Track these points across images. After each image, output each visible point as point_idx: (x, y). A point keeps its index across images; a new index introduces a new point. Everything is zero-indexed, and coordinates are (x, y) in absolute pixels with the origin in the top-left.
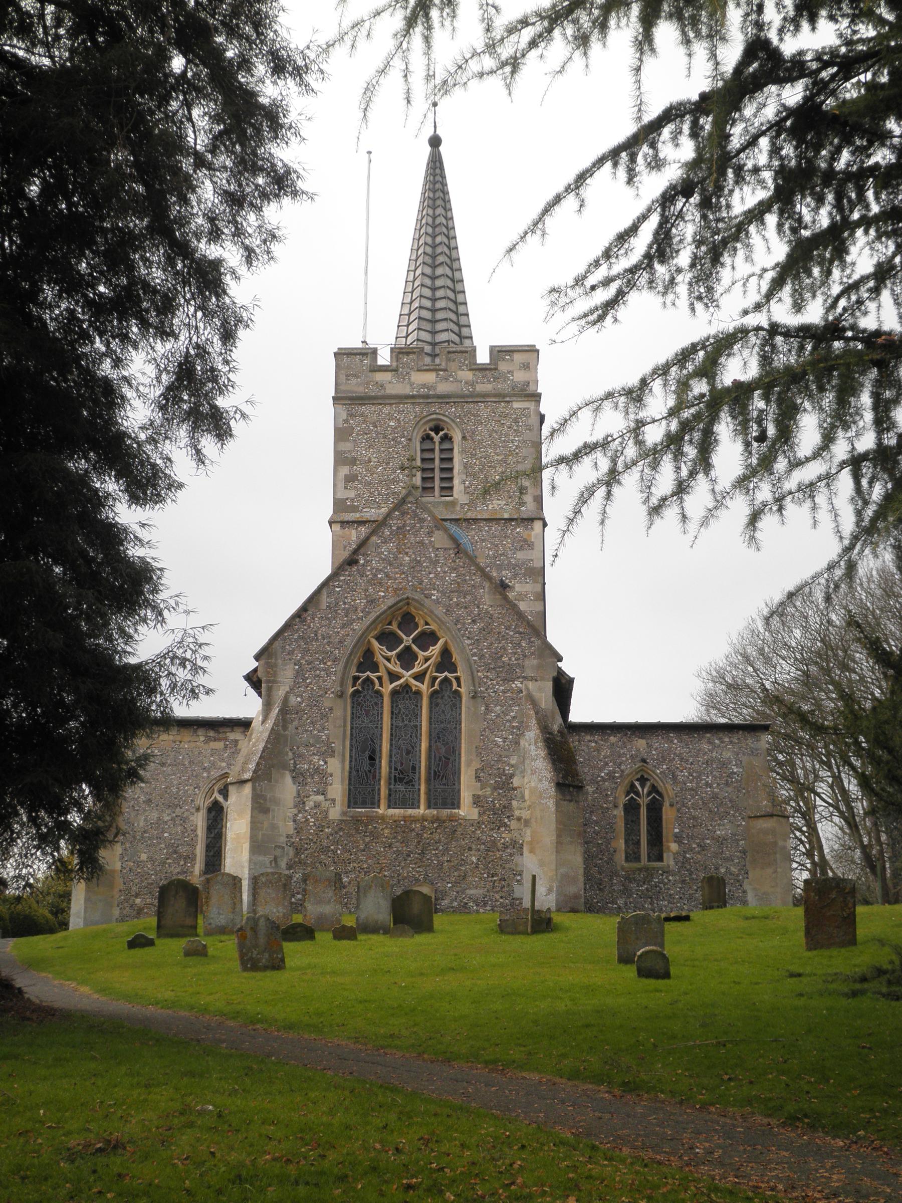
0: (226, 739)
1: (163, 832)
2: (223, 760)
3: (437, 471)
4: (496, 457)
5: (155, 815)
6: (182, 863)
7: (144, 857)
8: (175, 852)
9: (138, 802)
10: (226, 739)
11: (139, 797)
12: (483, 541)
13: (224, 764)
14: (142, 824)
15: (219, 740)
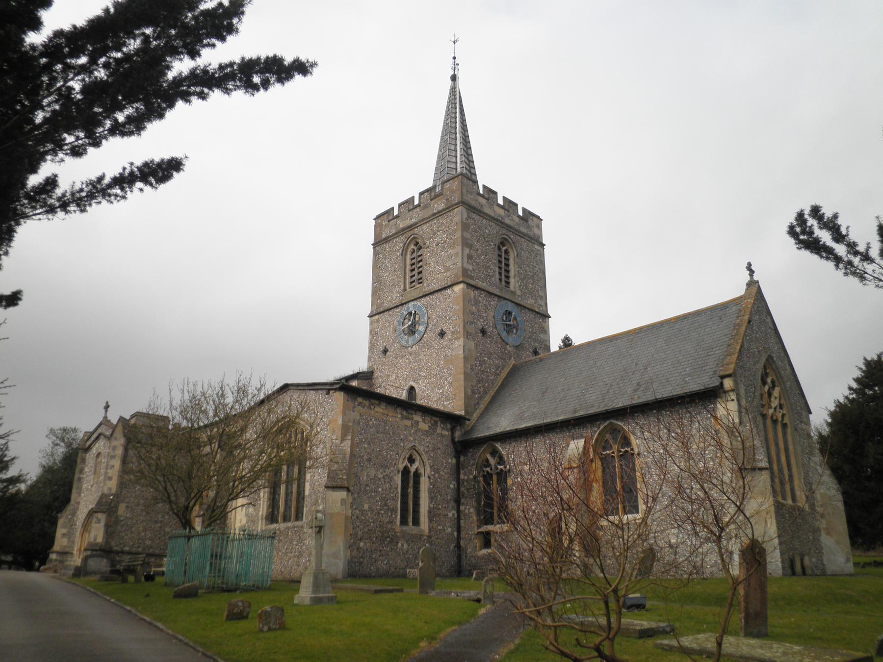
0: (412, 419)
1: (378, 487)
2: (411, 435)
3: (503, 270)
4: (530, 273)
5: (372, 472)
6: (390, 514)
7: (366, 507)
8: (386, 505)
9: (363, 459)
10: (412, 419)
11: (363, 456)
12: (527, 321)
13: (412, 439)
14: (365, 478)
15: (408, 419)
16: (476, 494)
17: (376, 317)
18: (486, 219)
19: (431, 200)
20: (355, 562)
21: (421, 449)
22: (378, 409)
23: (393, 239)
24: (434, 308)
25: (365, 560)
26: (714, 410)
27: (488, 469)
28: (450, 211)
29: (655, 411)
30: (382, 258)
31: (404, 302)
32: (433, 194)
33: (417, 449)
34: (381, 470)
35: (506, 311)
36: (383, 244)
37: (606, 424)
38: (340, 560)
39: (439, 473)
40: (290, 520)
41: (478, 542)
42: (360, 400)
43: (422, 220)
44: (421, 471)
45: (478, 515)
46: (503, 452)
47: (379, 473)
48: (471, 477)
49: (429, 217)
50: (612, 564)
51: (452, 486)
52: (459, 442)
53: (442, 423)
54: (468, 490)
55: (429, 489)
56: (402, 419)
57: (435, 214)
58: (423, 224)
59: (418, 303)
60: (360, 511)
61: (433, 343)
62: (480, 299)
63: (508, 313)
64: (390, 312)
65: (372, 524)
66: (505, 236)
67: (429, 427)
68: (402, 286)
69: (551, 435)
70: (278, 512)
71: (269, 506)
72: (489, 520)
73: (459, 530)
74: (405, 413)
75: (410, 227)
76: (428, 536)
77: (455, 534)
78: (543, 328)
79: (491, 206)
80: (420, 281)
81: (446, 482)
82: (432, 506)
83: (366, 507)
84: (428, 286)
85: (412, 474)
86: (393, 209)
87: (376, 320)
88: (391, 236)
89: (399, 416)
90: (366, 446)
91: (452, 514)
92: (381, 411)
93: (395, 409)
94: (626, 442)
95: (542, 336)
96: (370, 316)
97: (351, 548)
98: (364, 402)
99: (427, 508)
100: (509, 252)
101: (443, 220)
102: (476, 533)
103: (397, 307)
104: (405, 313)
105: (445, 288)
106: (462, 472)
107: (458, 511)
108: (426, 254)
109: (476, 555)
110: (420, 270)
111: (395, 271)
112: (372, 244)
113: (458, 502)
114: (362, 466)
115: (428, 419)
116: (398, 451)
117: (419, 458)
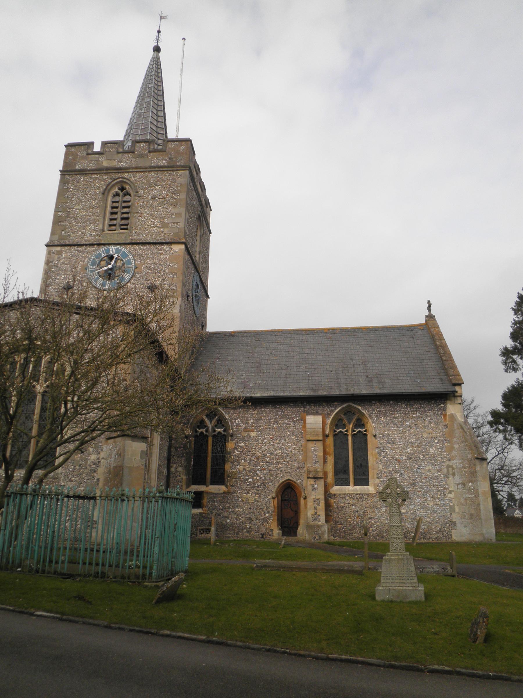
16: (187, 453)
19: (150, 152)
23: (92, 174)
24: (143, 259)
26: (444, 409)
27: (204, 430)
28: (173, 171)
29: (391, 402)
30: (73, 189)
31: (102, 242)
32: (152, 147)
36: (76, 174)
37: (344, 406)
43: (136, 168)
45: (187, 474)
46: (226, 417)
49: (146, 168)
50: (343, 528)
57: (154, 167)
59: (123, 249)
64: (80, 249)
68: (101, 226)
75: (119, 170)
80: (125, 227)
84: (138, 235)
86: (92, 143)
87: (58, 252)
88: (89, 170)
94: (360, 423)
96: (47, 246)
101: (165, 177)
103: (92, 245)
104: (103, 255)
105: (162, 243)
108: (138, 204)
111: (91, 207)
112: (61, 171)
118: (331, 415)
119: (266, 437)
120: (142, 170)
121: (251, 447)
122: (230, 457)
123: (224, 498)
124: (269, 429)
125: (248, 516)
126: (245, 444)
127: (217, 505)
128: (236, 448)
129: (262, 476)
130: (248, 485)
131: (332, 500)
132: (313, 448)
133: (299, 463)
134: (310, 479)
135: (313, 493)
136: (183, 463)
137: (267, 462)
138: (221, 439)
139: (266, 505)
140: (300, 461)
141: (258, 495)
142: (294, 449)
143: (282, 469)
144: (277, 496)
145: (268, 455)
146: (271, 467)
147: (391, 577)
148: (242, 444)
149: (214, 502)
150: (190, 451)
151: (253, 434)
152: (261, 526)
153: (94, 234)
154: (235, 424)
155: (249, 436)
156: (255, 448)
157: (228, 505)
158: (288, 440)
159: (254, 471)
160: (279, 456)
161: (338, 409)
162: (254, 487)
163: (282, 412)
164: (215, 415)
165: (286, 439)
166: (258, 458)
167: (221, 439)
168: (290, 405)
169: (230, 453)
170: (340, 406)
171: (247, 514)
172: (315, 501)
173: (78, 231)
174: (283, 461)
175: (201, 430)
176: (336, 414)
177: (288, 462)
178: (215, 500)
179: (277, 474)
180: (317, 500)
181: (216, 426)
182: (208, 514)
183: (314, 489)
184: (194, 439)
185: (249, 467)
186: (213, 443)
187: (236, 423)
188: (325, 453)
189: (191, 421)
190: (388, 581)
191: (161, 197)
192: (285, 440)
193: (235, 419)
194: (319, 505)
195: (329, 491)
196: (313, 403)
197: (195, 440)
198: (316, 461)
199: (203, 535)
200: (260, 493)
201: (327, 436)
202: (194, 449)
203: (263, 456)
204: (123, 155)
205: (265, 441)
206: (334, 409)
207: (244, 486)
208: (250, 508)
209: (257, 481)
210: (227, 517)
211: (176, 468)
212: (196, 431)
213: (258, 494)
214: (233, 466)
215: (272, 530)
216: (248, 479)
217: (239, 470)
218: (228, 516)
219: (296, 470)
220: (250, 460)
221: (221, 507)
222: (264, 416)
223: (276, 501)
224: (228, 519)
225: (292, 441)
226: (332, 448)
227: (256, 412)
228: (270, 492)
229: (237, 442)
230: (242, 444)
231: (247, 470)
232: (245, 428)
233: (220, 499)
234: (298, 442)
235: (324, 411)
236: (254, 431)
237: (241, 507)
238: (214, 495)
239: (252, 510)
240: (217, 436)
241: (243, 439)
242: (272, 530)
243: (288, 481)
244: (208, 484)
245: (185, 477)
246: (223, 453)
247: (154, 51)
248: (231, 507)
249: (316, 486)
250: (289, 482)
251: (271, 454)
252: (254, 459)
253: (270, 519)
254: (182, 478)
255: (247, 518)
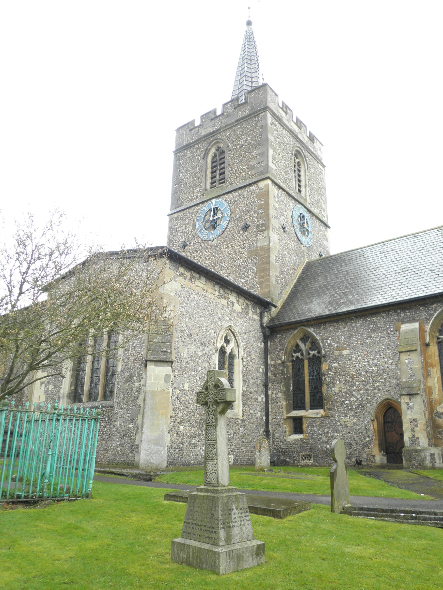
5: (193, 349)
7: (186, 386)
10: (228, 299)
13: (228, 319)
14: (186, 355)
15: (224, 298)
16: (285, 379)
17: (176, 215)
18: (286, 130)
19: (235, 108)
20: (175, 448)
21: (236, 329)
22: (198, 283)
23: (194, 145)
24: (237, 204)
25: (185, 445)
27: (299, 354)
33: (232, 329)
34: (201, 348)
35: (301, 214)
38: (164, 447)
39: (250, 356)
40: (95, 399)
41: (287, 427)
42: (182, 270)
44: (236, 352)
45: (287, 399)
46: (317, 337)
47: (199, 350)
48: (279, 362)
51: (261, 370)
52: (268, 327)
53: (253, 307)
54: (275, 375)
55: (242, 372)
56: (219, 298)
58: (227, 129)
60: (180, 390)
61: (236, 237)
62: (282, 198)
63: (302, 217)
64: (191, 210)
65: (192, 406)
66: (299, 149)
67: (242, 309)
68: (204, 187)
69: (375, 319)
70: (83, 390)
71: (71, 382)
72: (300, 406)
73: (267, 415)
74: (222, 292)
76: (241, 420)
77: (264, 418)
78: (326, 236)
79: (288, 120)
80: (222, 181)
81: (256, 366)
82: (245, 389)
83: (186, 386)
85: (227, 355)
86: (194, 121)
87: (176, 218)
88: (193, 143)
89: (217, 294)
90: (187, 320)
91: (261, 398)
92: (201, 285)
93: (214, 287)
95: (325, 242)
96: (168, 215)
97: (171, 433)
98: (186, 273)
99: (241, 392)
100: (300, 165)
102: (285, 418)
106: (269, 357)
107: (267, 396)
109: (285, 440)
110: (222, 171)
112: (174, 152)
113: (266, 386)
114: (183, 342)
115: (241, 301)
116: (216, 330)
117: (234, 339)
118: (430, 320)
119: (359, 354)
120: (230, 126)
121: (345, 367)
122: (325, 379)
123: (322, 423)
124: (361, 346)
125: (347, 441)
126: (339, 364)
127: (316, 430)
128: (330, 369)
129: (358, 397)
130: (345, 408)
131: (441, 420)
132: (407, 361)
133: (398, 380)
134: (404, 396)
135: (409, 412)
136: (282, 388)
137: (363, 381)
138: (316, 361)
139: (366, 428)
140: (399, 377)
141: (356, 418)
142: (391, 364)
143: (379, 387)
144: (376, 418)
145: (363, 373)
146: (368, 387)
147: (192, 524)
148: (336, 365)
149: (313, 427)
150: (287, 376)
151: (345, 352)
152: (362, 452)
153: (199, 194)
154: (327, 344)
155: (342, 355)
156: (349, 367)
157: (326, 430)
158: (384, 354)
159: (350, 391)
160: (375, 373)
161: (438, 312)
162: (351, 409)
163: (374, 324)
164: (309, 338)
165: (381, 354)
166: (352, 378)
167: (316, 361)
168: (382, 316)
169: (324, 375)
170: (440, 308)
171: (347, 439)
172: (411, 422)
173: (188, 197)
174: (379, 378)
175: (297, 354)
176: (435, 318)
177: (385, 379)
178: (314, 424)
179: (374, 394)
180: (414, 420)
181: (310, 349)
182: (308, 439)
183: (409, 408)
184: (291, 364)
185: (344, 388)
186: (309, 366)
187: (328, 343)
188: (426, 365)
189: (286, 346)
190: (189, 531)
191: (247, 144)
192: (380, 355)
193: (327, 339)
194: (416, 426)
195: (436, 409)
196: (408, 309)
197: (293, 365)
198: (411, 375)
199: (305, 461)
200: (358, 416)
201: (427, 345)
202: (293, 373)
203: (358, 375)
204: (215, 120)
205: (359, 358)
206: (433, 312)
207: (342, 409)
208: (349, 433)
209: (354, 403)
210: (327, 443)
211: (276, 394)
212: (293, 356)
213: (356, 416)
214: (328, 388)
215: (373, 456)
216: (345, 401)
217: (335, 392)
218: (328, 441)
219: (395, 388)
220: (345, 381)
221: (320, 432)
222: (356, 332)
223: (375, 423)
224: (328, 444)
225: (387, 355)
226: (437, 358)
227: (346, 329)
228: (368, 414)
229: (331, 363)
230: (336, 365)
231: (343, 391)
232: (337, 347)
233: (318, 423)
234: (395, 355)
235: (422, 317)
236: (346, 349)
237: (340, 432)
238: (313, 420)
239: (351, 435)
240: (312, 359)
241: (336, 359)
242: (373, 456)
243: (387, 401)
244: (307, 408)
245: (284, 403)
246: (319, 376)
247: (247, 25)
248: (330, 431)
249: (411, 404)
250: (388, 402)
251: (366, 372)
252: (349, 379)
253: (370, 444)
254: (282, 404)
255: (346, 444)
